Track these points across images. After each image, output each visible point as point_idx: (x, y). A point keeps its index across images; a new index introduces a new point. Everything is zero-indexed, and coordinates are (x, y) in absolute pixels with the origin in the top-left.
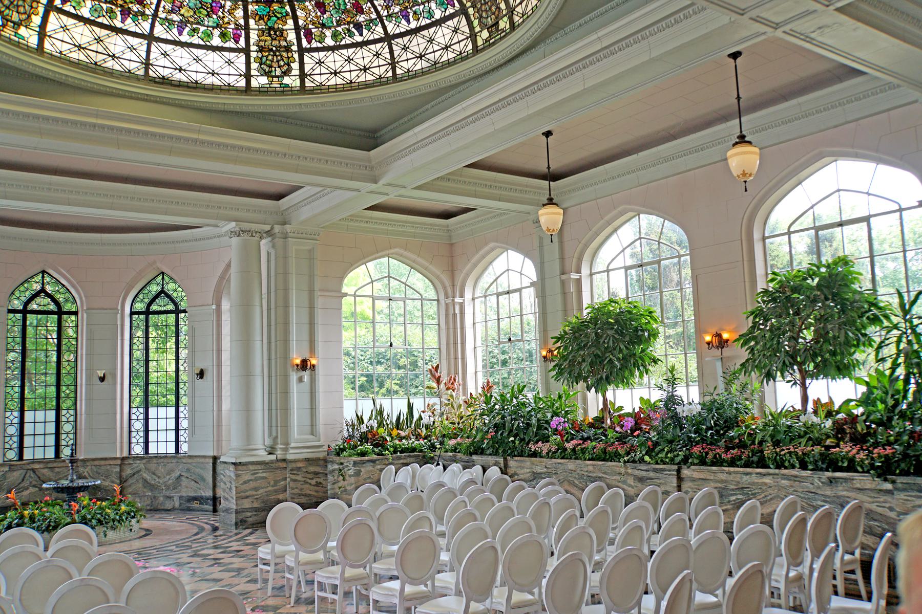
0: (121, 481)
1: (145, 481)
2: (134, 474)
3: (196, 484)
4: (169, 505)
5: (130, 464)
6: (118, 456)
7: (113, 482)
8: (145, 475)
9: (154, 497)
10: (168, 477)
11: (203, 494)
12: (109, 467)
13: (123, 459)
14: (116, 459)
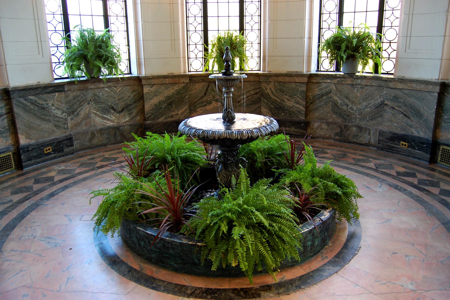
0: (307, 102)
1: (335, 104)
2: (322, 96)
3: (405, 119)
4: (365, 138)
5: (318, 83)
6: (305, 72)
7: (298, 103)
8: (336, 98)
9: (346, 126)
10: (365, 104)
11: (416, 134)
12: (293, 85)
13: (311, 76)
14: (302, 75)
